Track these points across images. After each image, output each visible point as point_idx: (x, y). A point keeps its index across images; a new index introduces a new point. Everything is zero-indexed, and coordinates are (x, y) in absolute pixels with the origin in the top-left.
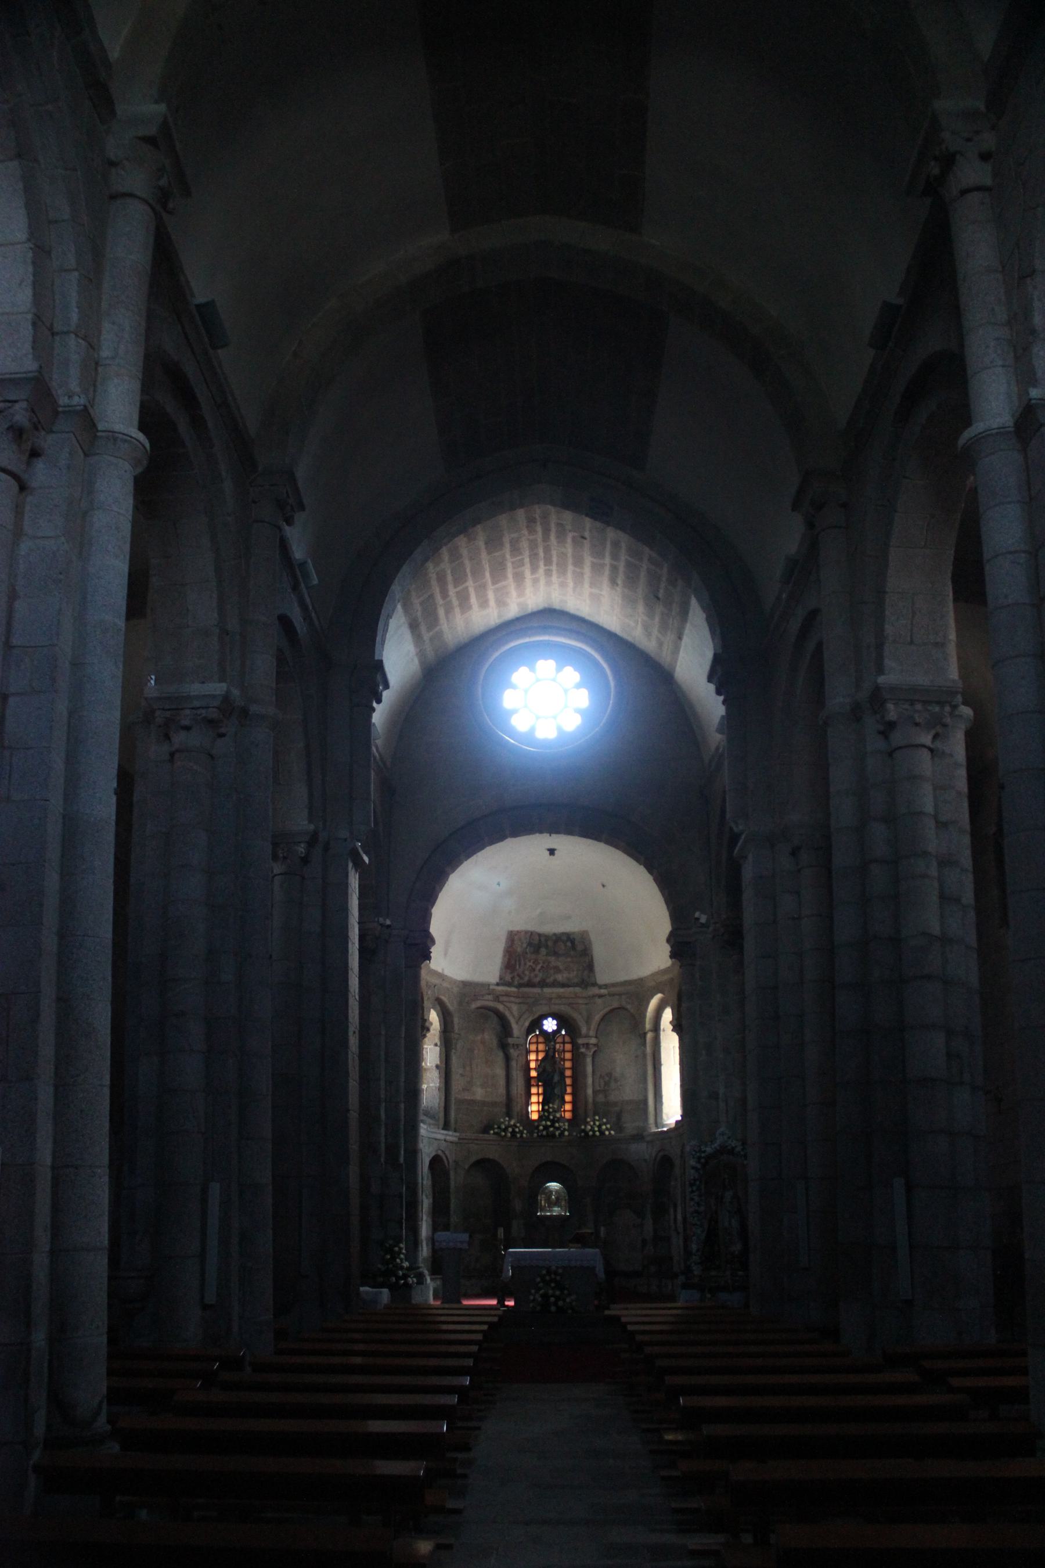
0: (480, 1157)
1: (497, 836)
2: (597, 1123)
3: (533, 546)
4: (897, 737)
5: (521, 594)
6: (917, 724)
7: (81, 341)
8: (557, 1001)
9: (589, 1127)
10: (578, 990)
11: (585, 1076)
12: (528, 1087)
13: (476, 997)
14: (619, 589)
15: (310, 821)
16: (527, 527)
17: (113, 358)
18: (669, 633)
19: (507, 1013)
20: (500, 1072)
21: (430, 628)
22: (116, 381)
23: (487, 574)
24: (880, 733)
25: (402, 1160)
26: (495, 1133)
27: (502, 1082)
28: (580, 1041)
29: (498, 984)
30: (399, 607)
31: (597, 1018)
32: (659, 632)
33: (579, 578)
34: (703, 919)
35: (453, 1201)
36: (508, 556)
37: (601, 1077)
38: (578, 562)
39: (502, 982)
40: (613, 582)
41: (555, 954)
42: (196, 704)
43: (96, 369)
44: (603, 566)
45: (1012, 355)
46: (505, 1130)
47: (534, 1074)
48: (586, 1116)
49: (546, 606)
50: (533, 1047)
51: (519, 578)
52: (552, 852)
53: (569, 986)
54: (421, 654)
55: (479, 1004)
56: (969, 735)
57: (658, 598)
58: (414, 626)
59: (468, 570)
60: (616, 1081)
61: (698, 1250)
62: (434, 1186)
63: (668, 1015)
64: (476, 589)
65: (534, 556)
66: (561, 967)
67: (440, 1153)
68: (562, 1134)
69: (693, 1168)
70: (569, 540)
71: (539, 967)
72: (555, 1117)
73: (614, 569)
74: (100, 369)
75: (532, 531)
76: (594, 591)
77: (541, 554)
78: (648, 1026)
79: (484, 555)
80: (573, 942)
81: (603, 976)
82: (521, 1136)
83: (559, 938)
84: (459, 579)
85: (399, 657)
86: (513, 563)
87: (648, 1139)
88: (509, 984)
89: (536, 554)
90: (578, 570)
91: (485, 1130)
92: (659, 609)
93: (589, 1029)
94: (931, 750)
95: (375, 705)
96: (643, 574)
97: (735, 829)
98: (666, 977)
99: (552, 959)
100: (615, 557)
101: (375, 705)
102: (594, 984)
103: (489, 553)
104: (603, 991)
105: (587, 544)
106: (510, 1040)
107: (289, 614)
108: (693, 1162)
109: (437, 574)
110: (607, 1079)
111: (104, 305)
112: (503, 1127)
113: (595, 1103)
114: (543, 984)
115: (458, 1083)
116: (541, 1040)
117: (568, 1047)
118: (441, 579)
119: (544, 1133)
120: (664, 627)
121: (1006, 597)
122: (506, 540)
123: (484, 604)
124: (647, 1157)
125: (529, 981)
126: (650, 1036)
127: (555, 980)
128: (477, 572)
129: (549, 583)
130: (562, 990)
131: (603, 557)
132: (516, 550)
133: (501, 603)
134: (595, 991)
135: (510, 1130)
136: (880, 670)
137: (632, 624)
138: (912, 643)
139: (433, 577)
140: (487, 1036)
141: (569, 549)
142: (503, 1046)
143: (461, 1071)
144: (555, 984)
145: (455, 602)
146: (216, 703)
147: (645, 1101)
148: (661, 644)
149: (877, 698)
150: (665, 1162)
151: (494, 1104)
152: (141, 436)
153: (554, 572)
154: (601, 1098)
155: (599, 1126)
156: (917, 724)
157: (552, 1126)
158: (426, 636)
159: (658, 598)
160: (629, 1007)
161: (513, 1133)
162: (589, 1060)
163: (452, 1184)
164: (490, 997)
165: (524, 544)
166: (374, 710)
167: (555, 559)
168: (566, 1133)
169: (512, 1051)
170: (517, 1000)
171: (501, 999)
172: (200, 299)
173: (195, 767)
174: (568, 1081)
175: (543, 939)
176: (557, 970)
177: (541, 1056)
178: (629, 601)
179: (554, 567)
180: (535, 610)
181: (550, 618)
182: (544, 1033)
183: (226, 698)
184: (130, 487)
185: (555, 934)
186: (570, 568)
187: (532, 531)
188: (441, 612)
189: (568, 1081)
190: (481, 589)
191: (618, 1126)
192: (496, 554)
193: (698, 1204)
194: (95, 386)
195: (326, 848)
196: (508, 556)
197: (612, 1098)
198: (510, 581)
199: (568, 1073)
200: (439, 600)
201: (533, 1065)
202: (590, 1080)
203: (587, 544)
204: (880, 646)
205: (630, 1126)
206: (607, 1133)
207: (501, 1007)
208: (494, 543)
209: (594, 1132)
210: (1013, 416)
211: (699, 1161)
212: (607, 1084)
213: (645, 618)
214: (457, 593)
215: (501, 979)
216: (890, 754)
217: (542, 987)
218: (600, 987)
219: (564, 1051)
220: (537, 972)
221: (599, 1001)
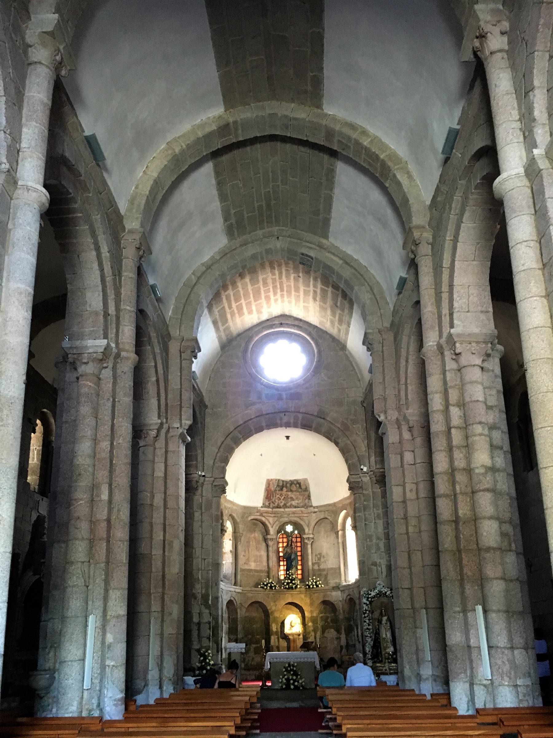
0: (254, 600)
1: (259, 429)
2: (315, 581)
3: (274, 281)
4: (463, 360)
5: (269, 307)
6: (473, 354)
7: (7, 135)
8: (293, 515)
9: (310, 583)
10: (303, 509)
11: (307, 555)
12: (279, 561)
13: (250, 514)
14: (318, 303)
15: (159, 417)
16: (271, 272)
17: (29, 148)
18: (343, 324)
19: (267, 523)
20: (264, 553)
21: (223, 325)
22: (29, 160)
23: (251, 296)
24: (454, 359)
25: (210, 602)
26: (261, 587)
27: (265, 558)
28: (305, 536)
29: (262, 507)
30: (206, 311)
31: (313, 523)
32: (338, 324)
33: (297, 298)
34: (365, 469)
35: (239, 626)
36: (262, 287)
37: (316, 555)
38: (297, 289)
39: (264, 506)
40: (315, 299)
41: (291, 491)
42: (91, 350)
43: (18, 153)
44: (309, 291)
45: (522, 136)
46: (266, 585)
47: (281, 554)
48: (309, 576)
49: (282, 313)
50: (281, 540)
51: (268, 298)
52: (288, 437)
53: (298, 507)
54: (219, 338)
55: (252, 517)
56: (500, 359)
57: (337, 306)
58: (215, 323)
59: (242, 295)
61: (369, 651)
62: (229, 617)
63: (349, 521)
64: (246, 304)
65: (275, 287)
66: (294, 498)
67: (232, 599)
68: (296, 587)
69: (365, 603)
70: (292, 278)
71: (283, 497)
72: (292, 578)
73: (315, 292)
74: (20, 153)
75: (274, 274)
76: (306, 304)
77: (279, 286)
78: (339, 528)
79: (250, 287)
80: (300, 484)
81: (315, 502)
82: (275, 589)
83: (292, 483)
84: (237, 300)
85: (208, 339)
86: (264, 290)
87: (341, 589)
88: (269, 507)
89: (276, 286)
90: (298, 294)
91: (256, 585)
92: (338, 312)
93: (309, 530)
94: (482, 368)
95: (193, 359)
96: (329, 294)
97: (380, 420)
98: (348, 501)
99: (289, 493)
100: (315, 286)
101: (193, 359)
102: (311, 506)
103: (252, 285)
104: (316, 510)
105: (301, 280)
106: (269, 537)
107: (145, 309)
108: (364, 600)
109: (226, 296)
110: (319, 556)
111: (24, 120)
112: (265, 583)
113: (313, 569)
114: (285, 506)
115: (241, 561)
116: (285, 536)
117: (299, 540)
118: (228, 298)
119: (287, 587)
120: (341, 321)
121: (523, 265)
122: (261, 278)
123: (250, 312)
124: (341, 599)
125: (278, 505)
126: (340, 533)
127: (291, 504)
128: (246, 296)
129: (283, 301)
130: (295, 509)
131: (309, 286)
132: (265, 284)
133: (259, 312)
134: (312, 509)
135: (269, 585)
136: (452, 326)
137: (325, 321)
138: (468, 312)
139: (224, 298)
140: (256, 535)
141: (292, 284)
142: (265, 540)
143: (243, 553)
144: (290, 507)
145: (236, 311)
146: (102, 350)
147: (339, 568)
148: (339, 330)
149: (451, 341)
150: (351, 601)
151: (261, 571)
152: (44, 190)
153: (285, 296)
154: (316, 567)
155: (316, 582)
156: (473, 354)
157: (291, 582)
158: (221, 328)
159: (337, 306)
160: (329, 518)
161: (271, 587)
162: (309, 546)
163: (239, 617)
164: (258, 514)
165: (270, 281)
166: (193, 362)
167: (285, 289)
168: (299, 586)
169: (269, 542)
170: (273, 515)
171: (264, 515)
172: (87, 133)
173: (90, 384)
174: (299, 558)
175: (285, 483)
176: (292, 499)
177: (285, 544)
178: (323, 309)
179: (285, 293)
180: (276, 315)
181: (284, 320)
182: (286, 533)
183: (107, 348)
184: (37, 217)
185: (291, 481)
186: (293, 293)
187: (274, 274)
188: (229, 316)
189: (299, 558)
190: (249, 304)
191: (326, 583)
192: (256, 286)
193: (369, 625)
194: (17, 162)
195: (168, 431)
196: (262, 287)
198: (263, 301)
199: (299, 554)
200: (227, 310)
201: (281, 550)
202: (310, 557)
203: (301, 280)
204: (451, 315)
205: (332, 582)
206: (320, 586)
207: (263, 519)
208: (254, 281)
209: (313, 585)
210: (524, 167)
211: (367, 600)
212: (319, 559)
213: (332, 317)
214: (237, 306)
215: (263, 504)
216: (459, 370)
217: (284, 508)
218: (314, 508)
219: (297, 542)
220: (282, 500)
221: (314, 515)
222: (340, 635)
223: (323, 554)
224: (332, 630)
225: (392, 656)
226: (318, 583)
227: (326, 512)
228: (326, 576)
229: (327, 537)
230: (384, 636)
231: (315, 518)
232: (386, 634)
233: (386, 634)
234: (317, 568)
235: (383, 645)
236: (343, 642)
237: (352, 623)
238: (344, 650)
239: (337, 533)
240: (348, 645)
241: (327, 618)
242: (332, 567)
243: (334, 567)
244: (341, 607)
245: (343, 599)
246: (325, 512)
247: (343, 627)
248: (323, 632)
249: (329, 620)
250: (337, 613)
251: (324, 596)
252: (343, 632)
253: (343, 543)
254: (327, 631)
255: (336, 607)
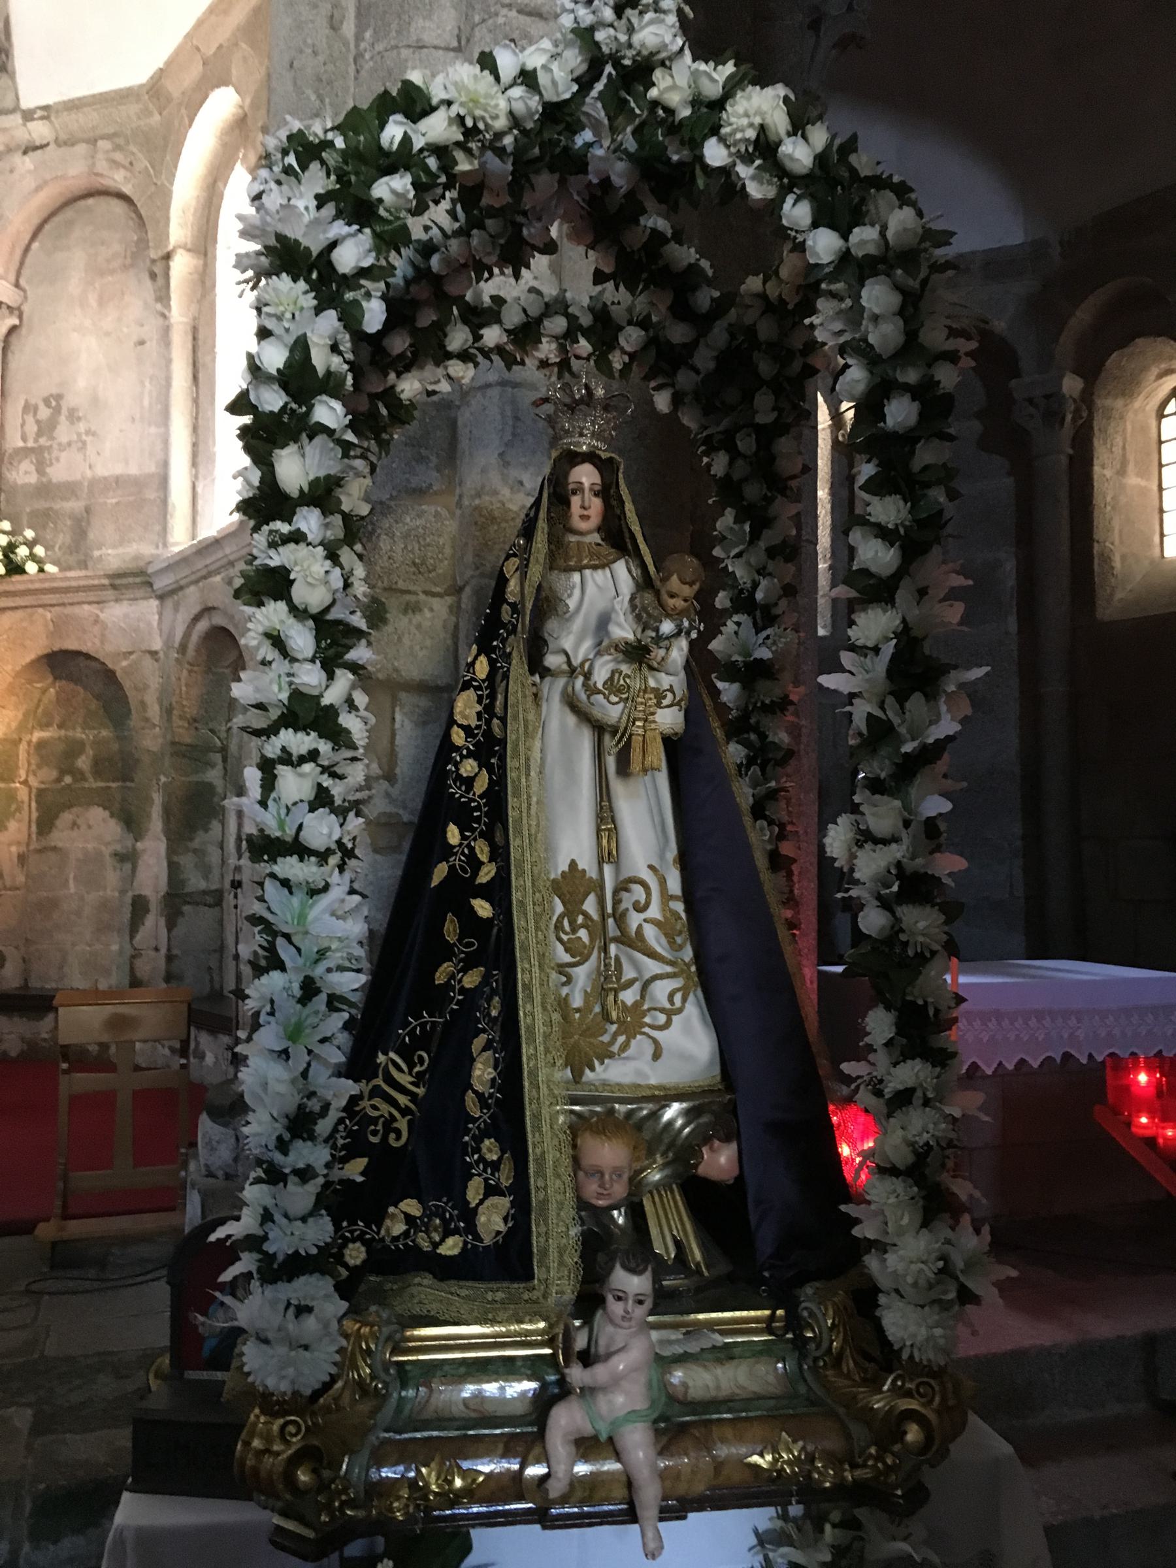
37: (28, 408)
60: (73, 417)
78: (179, 229)
87: (160, 584)
110: (44, 413)
124: (157, 644)
126: (181, 266)
147: (163, 481)
193: (333, 639)
197: (58, 473)
206: (31, 568)
212: (47, 428)
222: (138, 837)
223: (70, 401)
224: (97, 814)
225: (682, 1157)
226: (23, 551)
227: (103, 145)
228: (80, 527)
229: (101, 302)
230: (574, 845)
231: (30, 183)
232: (605, 817)
233: (605, 817)
234: (33, 479)
235: (554, 974)
236: (152, 875)
237: (214, 775)
238: (154, 923)
239: (158, 272)
240: (176, 900)
241: (73, 749)
242: (118, 469)
243: (133, 470)
244: (154, 682)
245: (168, 644)
246: (93, 142)
247: (157, 798)
248: (45, 824)
249: (83, 762)
250: (134, 721)
251: (58, 626)
252: (156, 824)
253: (195, 331)
254: (66, 817)
255: (127, 684)
